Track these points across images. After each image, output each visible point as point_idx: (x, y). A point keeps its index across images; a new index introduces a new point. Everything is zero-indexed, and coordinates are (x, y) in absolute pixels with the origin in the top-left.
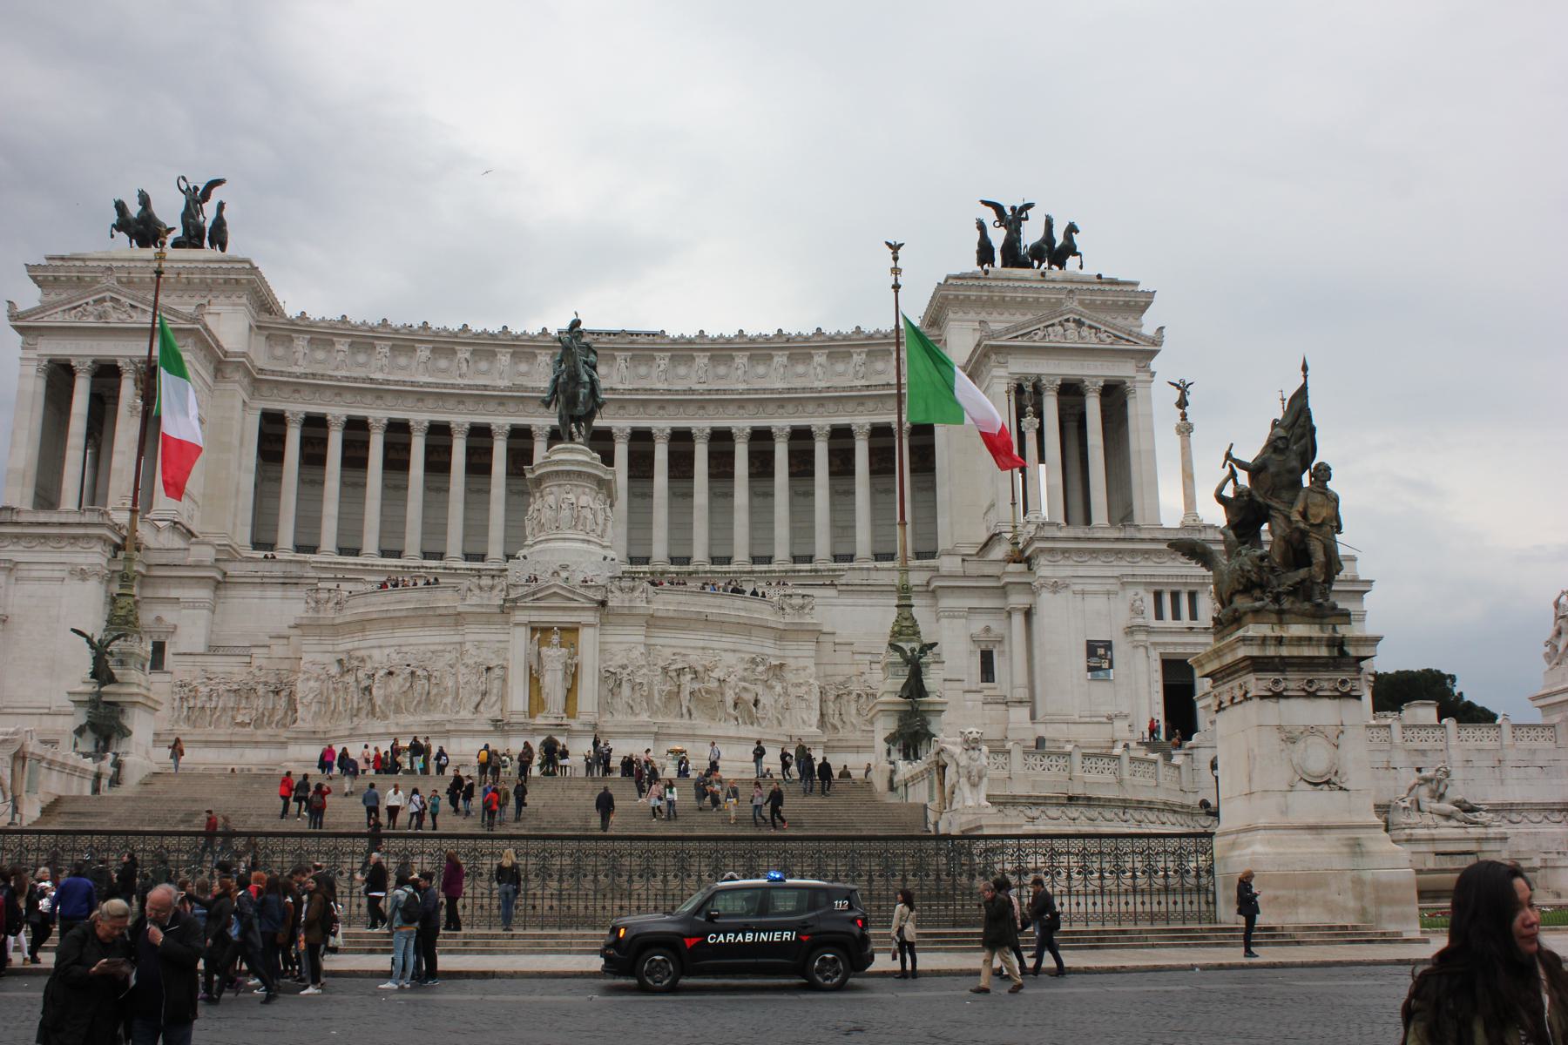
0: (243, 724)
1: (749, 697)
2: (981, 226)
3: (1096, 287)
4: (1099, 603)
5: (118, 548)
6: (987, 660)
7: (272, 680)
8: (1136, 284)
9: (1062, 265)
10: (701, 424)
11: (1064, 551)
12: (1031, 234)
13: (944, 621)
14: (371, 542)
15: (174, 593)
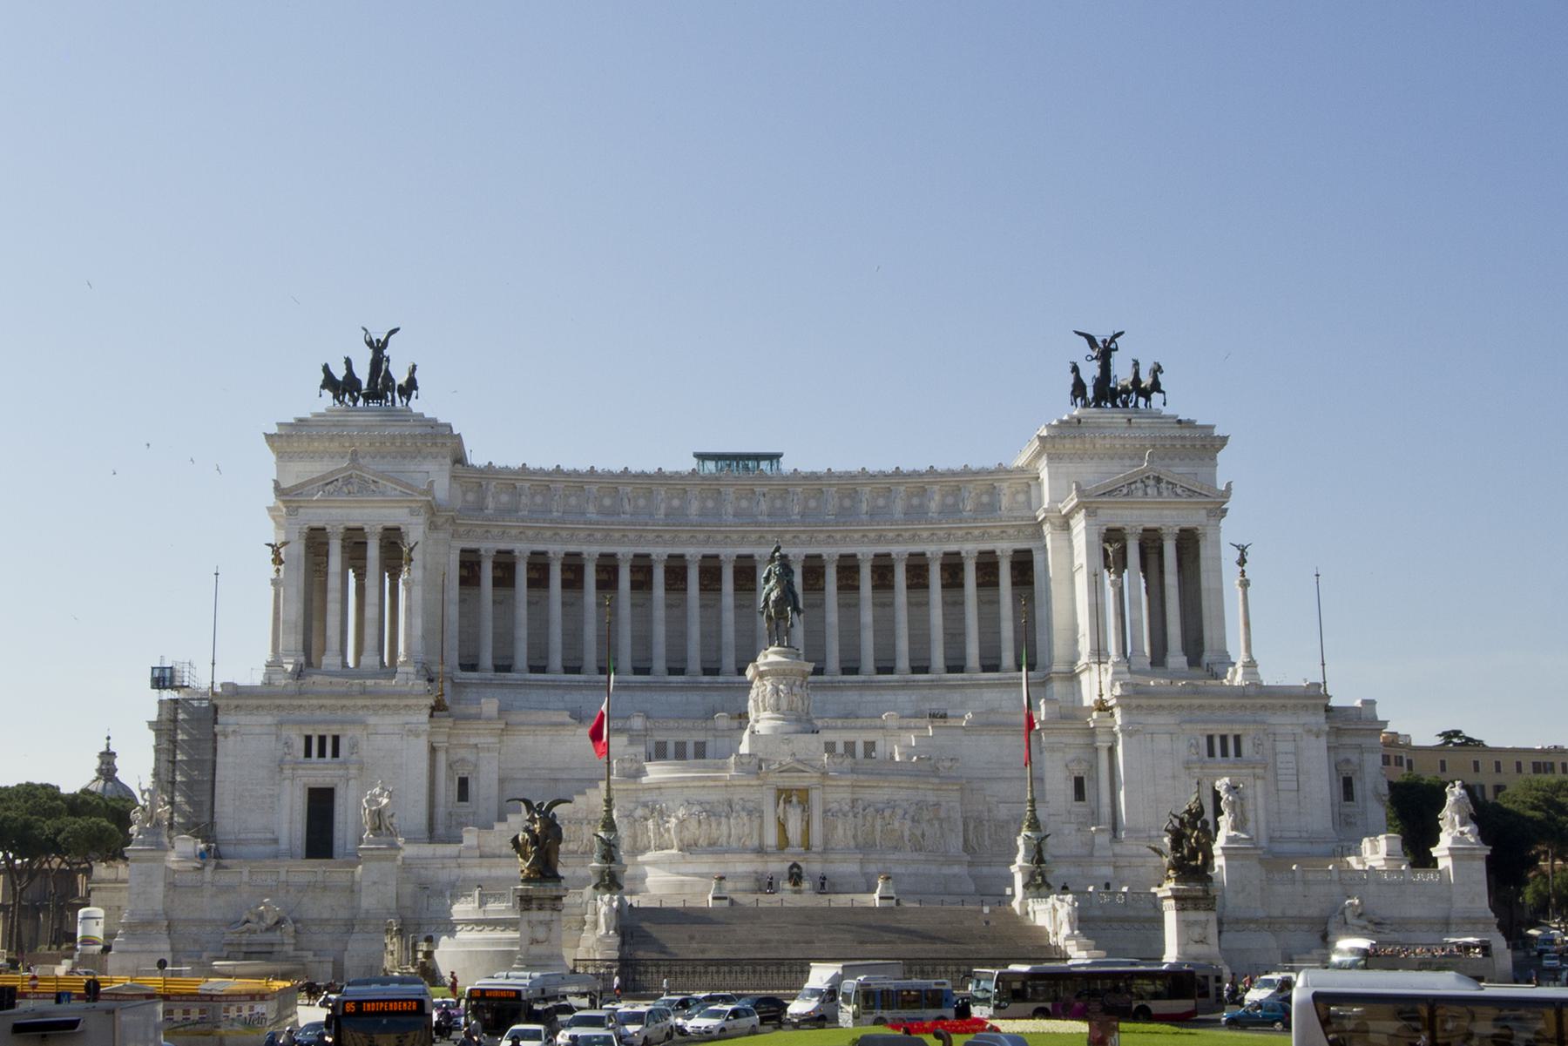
0: (575, 852)
1: (918, 833)
2: (1075, 369)
3: (1177, 432)
4: (1163, 742)
5: (433, 709)
6: (1079, 784)
7: (591, 817)
8: (1212, 427)
9: (1148, 399)
10: (831, 553)
11: (1138, 707)
12: (1122, 374)
13: (1046, 754)
14: (556, 661)
15: (473, 741)
